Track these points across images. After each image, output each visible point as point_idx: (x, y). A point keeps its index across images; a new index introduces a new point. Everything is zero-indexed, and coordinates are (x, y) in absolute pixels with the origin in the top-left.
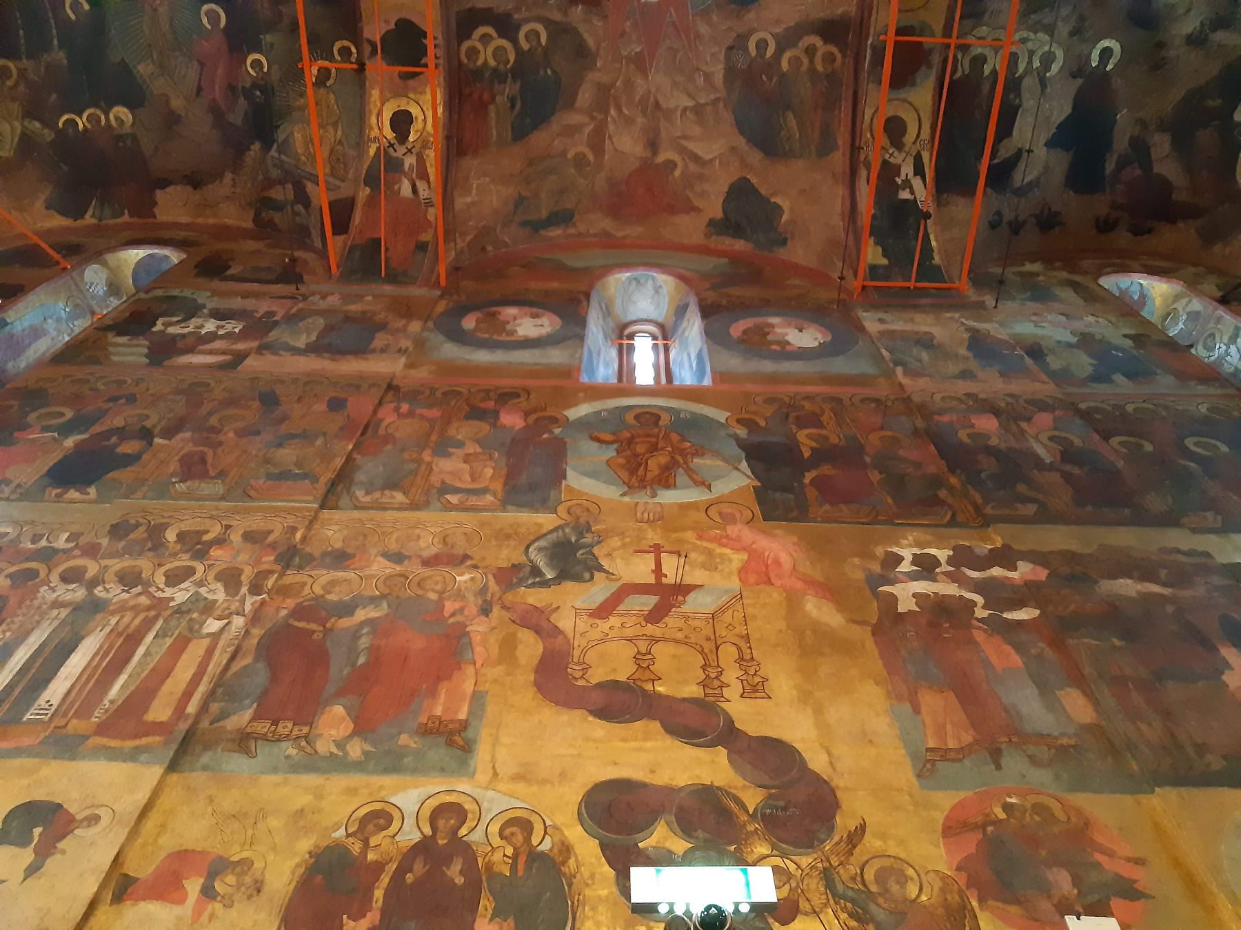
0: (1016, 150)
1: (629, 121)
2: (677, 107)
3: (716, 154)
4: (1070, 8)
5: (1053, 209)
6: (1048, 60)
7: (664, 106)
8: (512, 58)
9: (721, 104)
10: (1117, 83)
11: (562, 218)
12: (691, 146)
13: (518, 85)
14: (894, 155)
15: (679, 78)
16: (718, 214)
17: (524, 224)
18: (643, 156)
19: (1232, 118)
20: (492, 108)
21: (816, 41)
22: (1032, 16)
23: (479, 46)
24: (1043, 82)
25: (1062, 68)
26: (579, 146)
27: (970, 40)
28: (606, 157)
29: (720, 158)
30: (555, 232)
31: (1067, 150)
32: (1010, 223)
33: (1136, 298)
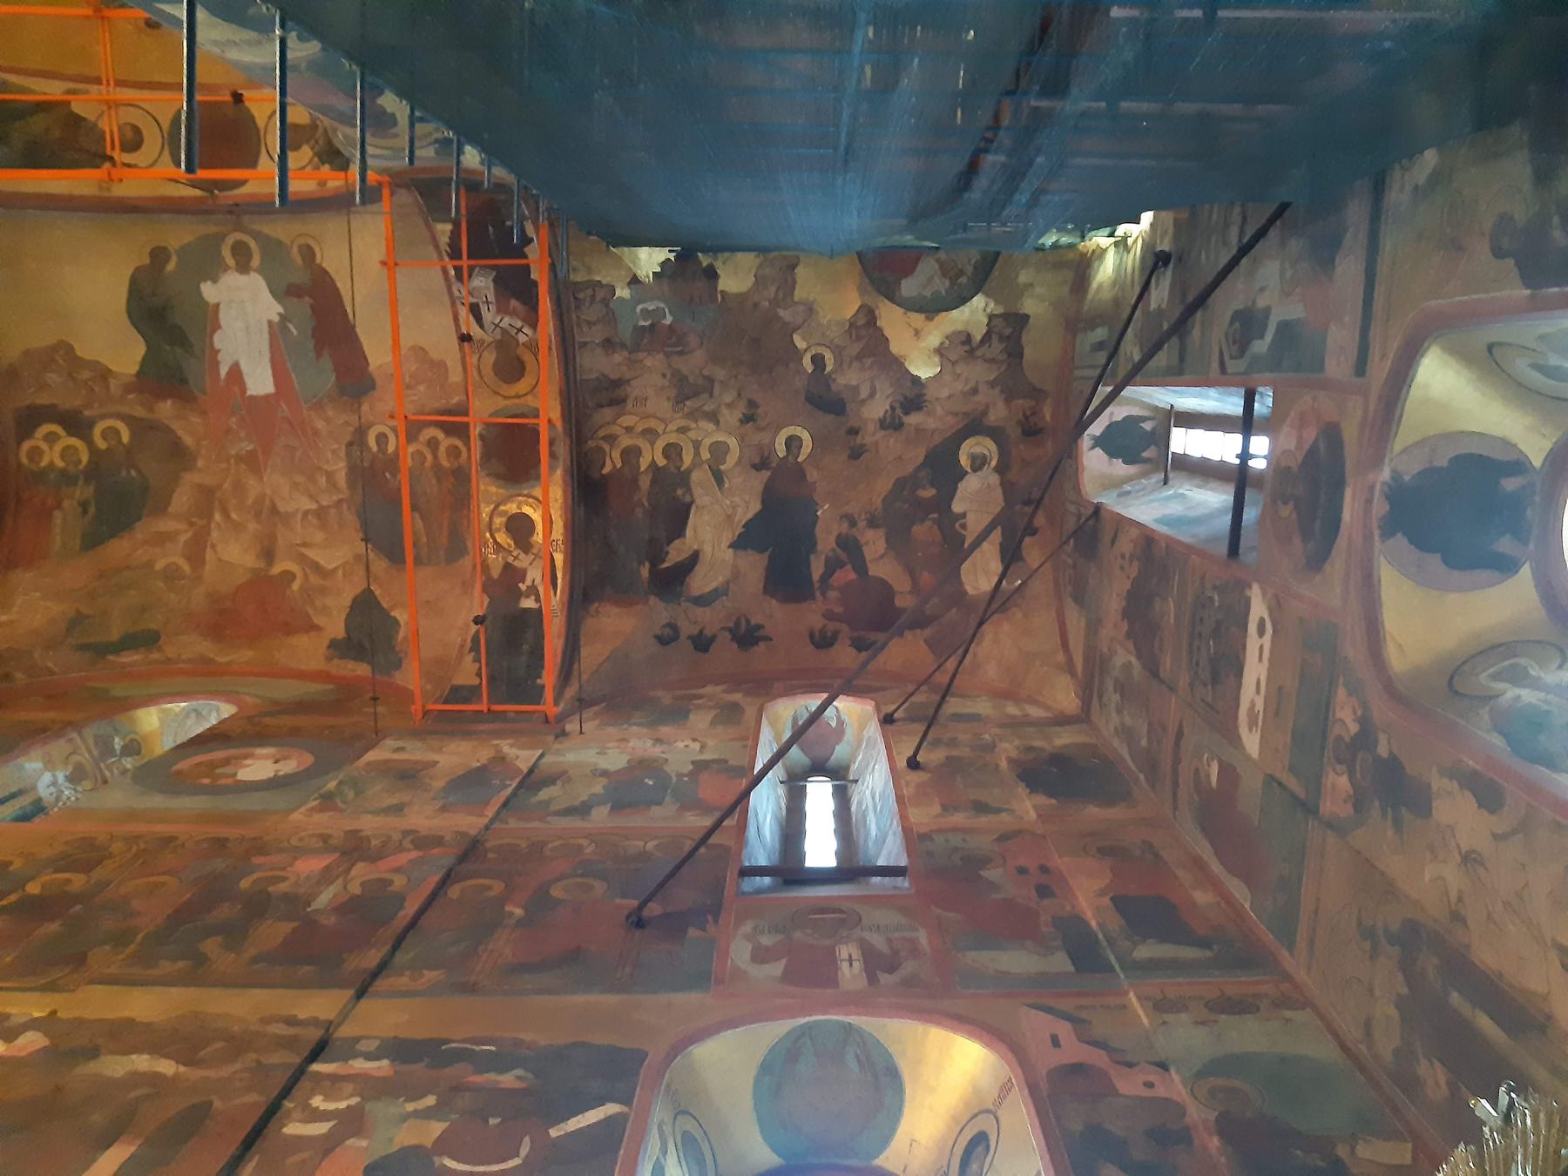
0: (690, 553)
1: (238, 527)
2: (297, 510)
3: (339, 563)
4: (735, 393)
5: (753, 622)
6: (719, 450)
7: (282, 510)
8: (85, 458)
9: (345, 506)
10: (812, 475)
11: (148, 640)
12: (312, 554)
13: (91, 489)
14: (520, 557)
15: (300, 479)
16: (340, 632)
17: (84, 647)
18: (257, 566)
19: (952, 512)
20: (58, 515)
21: (440, 435)
22: (688, 403)
23: (44, 446)
24: (719, 477)
25: (740, 458)
26: (173, 556)
27: (616, 429)
28: (207, 568)
29: (344, 568)
30: (130, 658)
31: (761, 551)
32: (690, 637)
33: (834, 724)
